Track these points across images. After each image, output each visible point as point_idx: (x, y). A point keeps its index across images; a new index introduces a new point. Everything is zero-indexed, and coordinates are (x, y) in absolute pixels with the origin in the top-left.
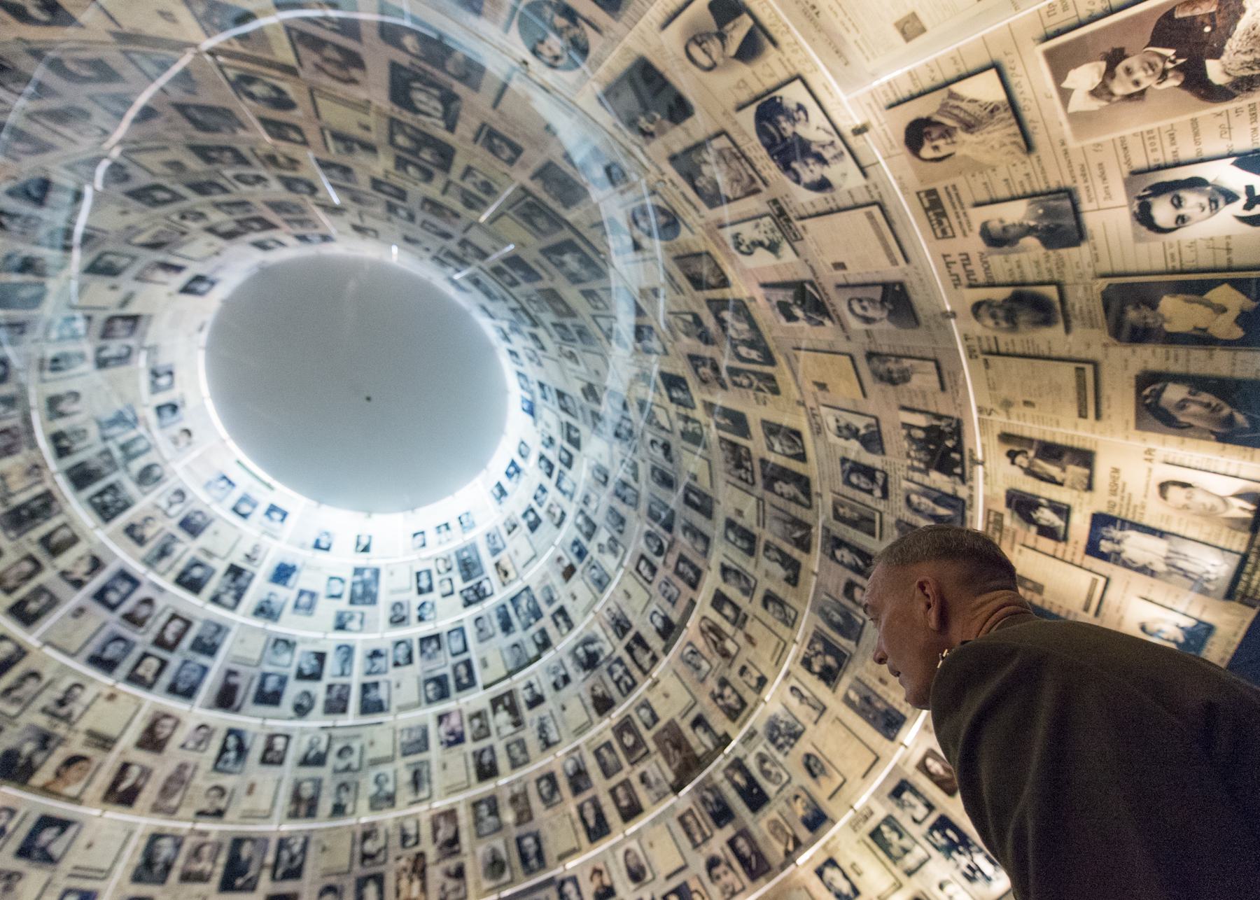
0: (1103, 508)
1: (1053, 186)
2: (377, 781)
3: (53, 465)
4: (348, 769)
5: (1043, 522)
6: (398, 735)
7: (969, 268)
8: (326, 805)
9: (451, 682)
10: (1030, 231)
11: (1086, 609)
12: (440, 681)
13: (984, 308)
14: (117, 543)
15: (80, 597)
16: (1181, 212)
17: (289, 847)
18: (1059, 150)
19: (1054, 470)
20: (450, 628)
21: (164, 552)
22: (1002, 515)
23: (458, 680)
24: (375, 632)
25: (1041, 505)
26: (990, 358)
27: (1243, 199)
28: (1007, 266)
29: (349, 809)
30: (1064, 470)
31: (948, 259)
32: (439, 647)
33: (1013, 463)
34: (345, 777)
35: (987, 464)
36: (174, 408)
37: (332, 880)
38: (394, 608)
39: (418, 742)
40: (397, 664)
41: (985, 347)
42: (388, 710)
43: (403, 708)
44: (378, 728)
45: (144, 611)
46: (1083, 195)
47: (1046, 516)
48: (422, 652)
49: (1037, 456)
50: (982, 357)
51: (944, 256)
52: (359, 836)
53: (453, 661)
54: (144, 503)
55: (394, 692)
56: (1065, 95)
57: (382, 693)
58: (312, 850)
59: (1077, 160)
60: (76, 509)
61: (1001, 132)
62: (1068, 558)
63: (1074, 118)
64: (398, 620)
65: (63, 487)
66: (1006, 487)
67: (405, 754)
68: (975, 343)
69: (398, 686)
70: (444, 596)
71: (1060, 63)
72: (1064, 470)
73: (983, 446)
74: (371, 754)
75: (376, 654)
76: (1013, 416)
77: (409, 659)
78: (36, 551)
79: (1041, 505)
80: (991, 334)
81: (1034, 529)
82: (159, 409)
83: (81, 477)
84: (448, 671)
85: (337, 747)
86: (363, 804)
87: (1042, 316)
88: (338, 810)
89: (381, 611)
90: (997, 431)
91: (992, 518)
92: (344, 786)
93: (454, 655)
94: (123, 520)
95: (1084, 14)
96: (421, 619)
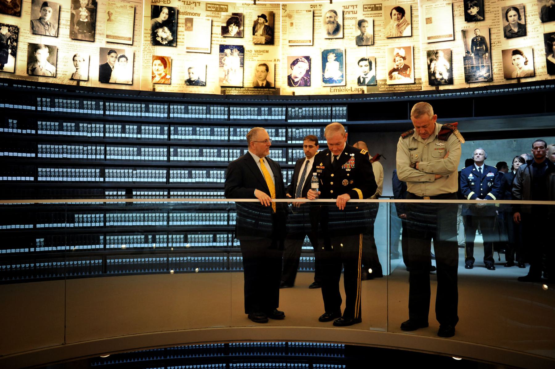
0: (246, 48)
1: (375, 42)
5: (230, 28)
7: (351, 13)
10: (363, 34)
11: (187, 48)
13: (335, 15)
16: (363, 66)
18: (386, 44)
19: (260, 31)
22: (227, 10)
25: (239, 27)
26: (312, 12)
27: (365, 77)
28: (351, 25)
30: (261, 35)
31: (355, 7)
33: (259, 17)
35: (254, 6)
41: (316, 12)
46: (371, 47)
47: (234, 30)
49: (266, 26)
50: (312, 10)
51: (356, 6)
56: (400, 48)
59: (382, 48)
61: (395, 33)
62: (213, 39)
63: (393, 49)
66: (244, 13)
68: (318, 7)
71: (407, 49)
72: (261, 35)
73: (265, 5)
76: (284, 18)
79: (239, 27)
80: (323, 15)
81: (225, 25)
87: (331, 32)
90: (275, 11)
91: (223, 7)
95: (415, 55)
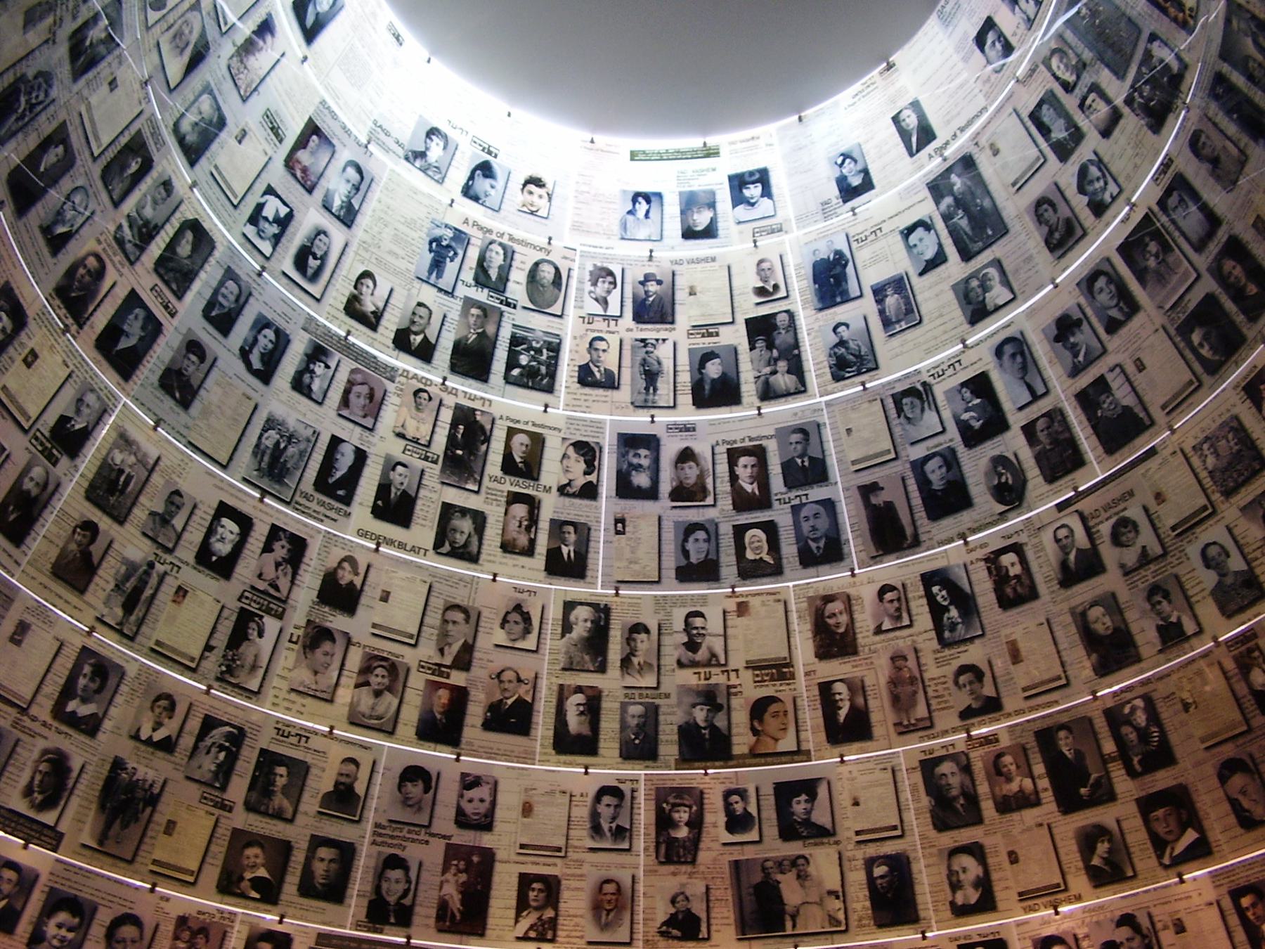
2: (1208, 562)
3: (435, 373)
4: (1145, 559)
6: (1196, 461)
8: (1145, 633)
9: (1229, 305)
12: (1207, 313)
14: (588, 409)
15: (607, 504)
17: (1128, 721)
20: (1158, 193)
21: (651, 376)
23: (1238, 295)
24: (1042, 292)
29: (1189, 627)
32: (1166, 248)
34: (1149, 575)
36: (485, 169)
37: (1228, 751)
38: (1040, 219)
39: (1237, 457)
40: (1113, 326)
42: (1153, 423)
43: (1175, 405)
44: (1152, 464)
45: (691, 472)
48: (1141, 276)
52: (1230, 665)
53: (1203, 261)
54: (570, 328)
55: (1139, 380)
57: (1122, 394)
58: (1165, 713)
60: (504, 403)
64: (1062, 238)
65: (465, 390)
67: (1228, 494)
69: (1140, 366)
70: (1106, 133)
74: (1168, 517)
75: (1065, 328)
77: (1133, 307)
78: (512, 485)
82: (468, 192)
83: (472, 360)
84: (1209, 285)
85: (1105, 529)
86: (1208, 611)
88: (1172, 636)
89: (1023, 241)
92: (1156, 592)
93: (1199, 247)
94: (566, 373)
96: (1099, 208)
